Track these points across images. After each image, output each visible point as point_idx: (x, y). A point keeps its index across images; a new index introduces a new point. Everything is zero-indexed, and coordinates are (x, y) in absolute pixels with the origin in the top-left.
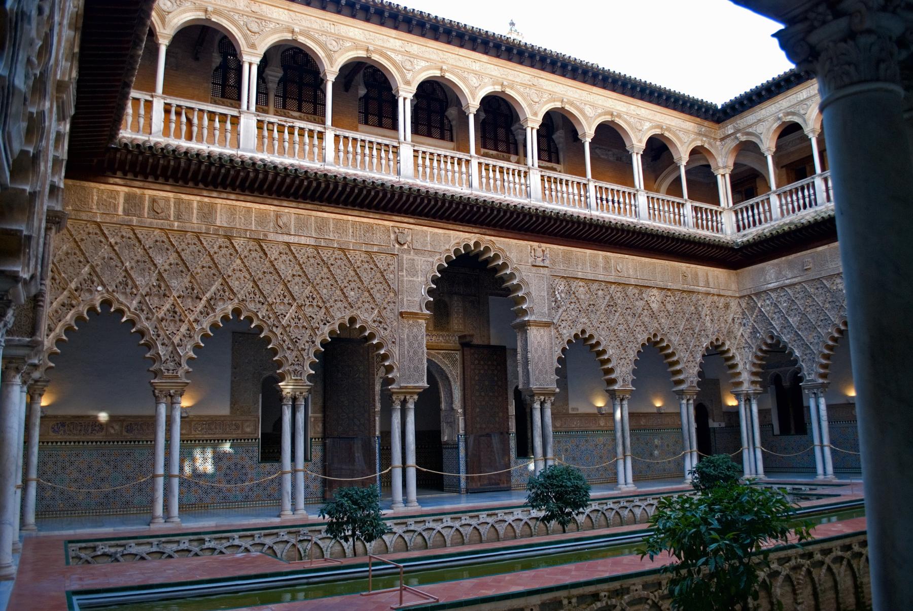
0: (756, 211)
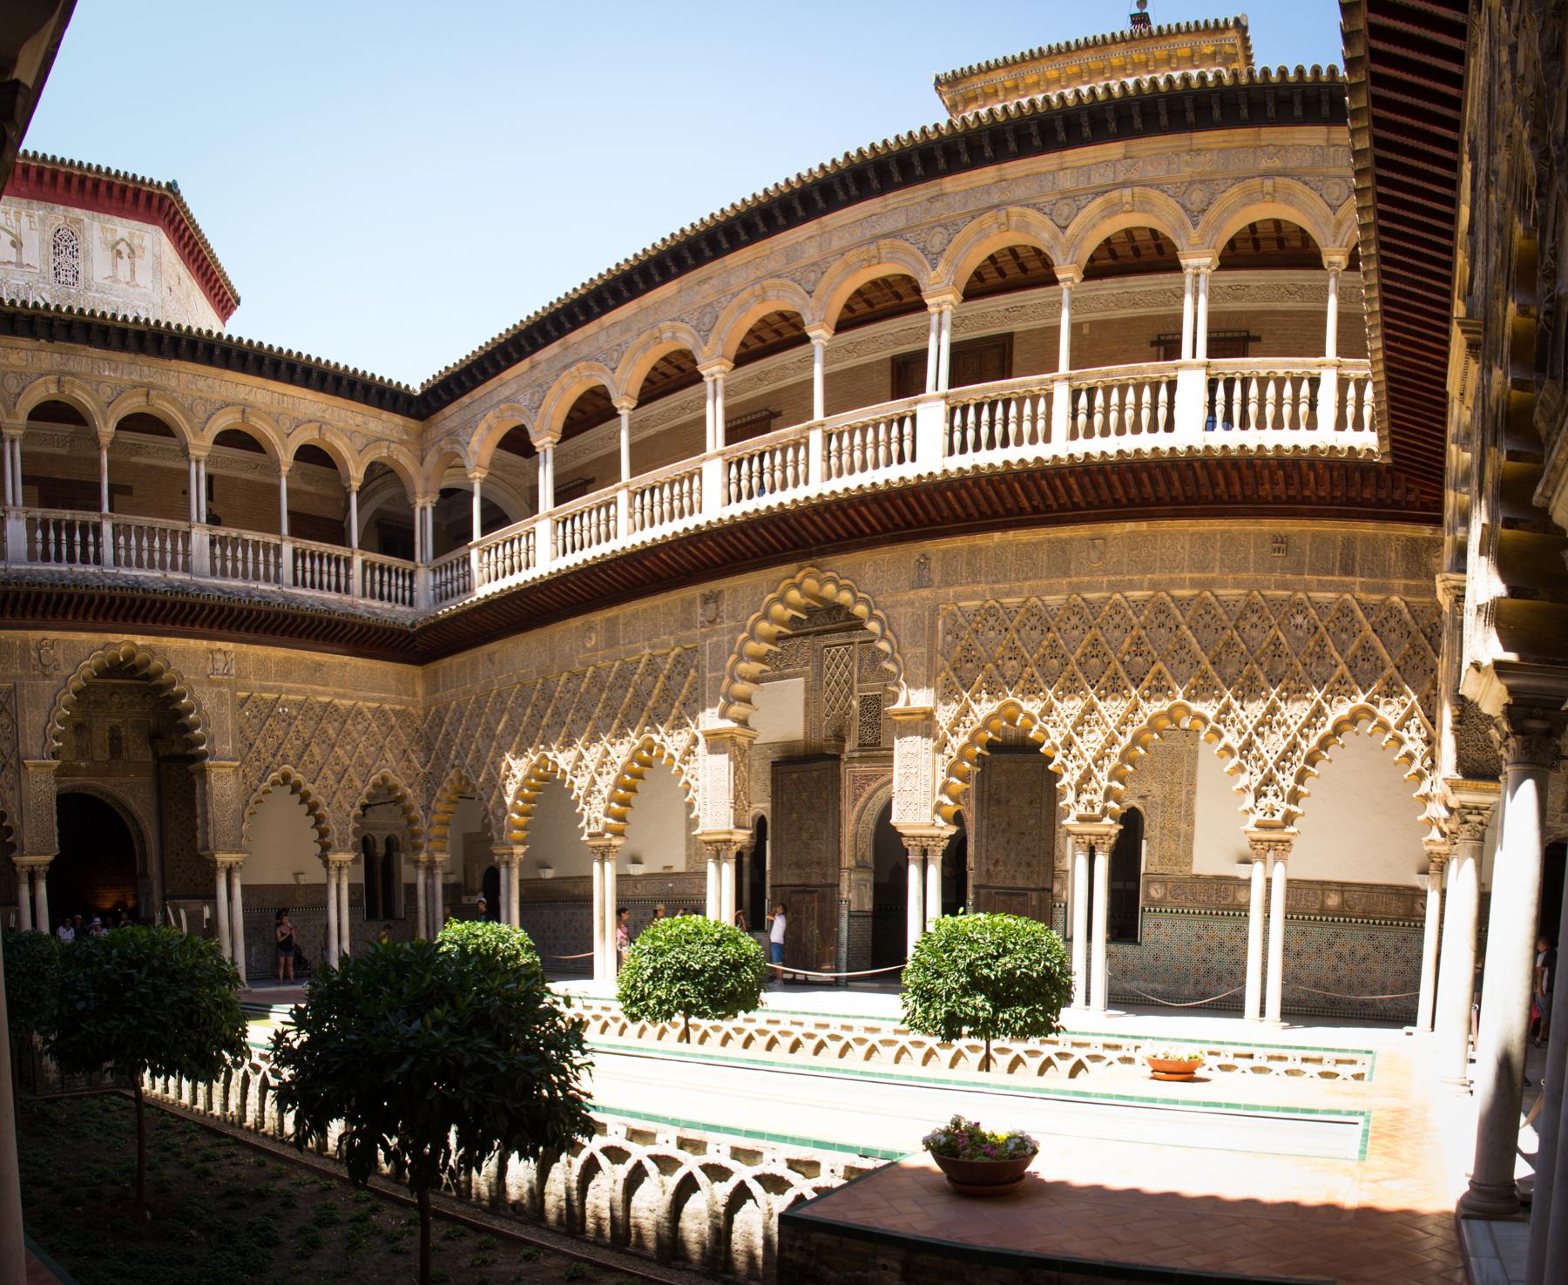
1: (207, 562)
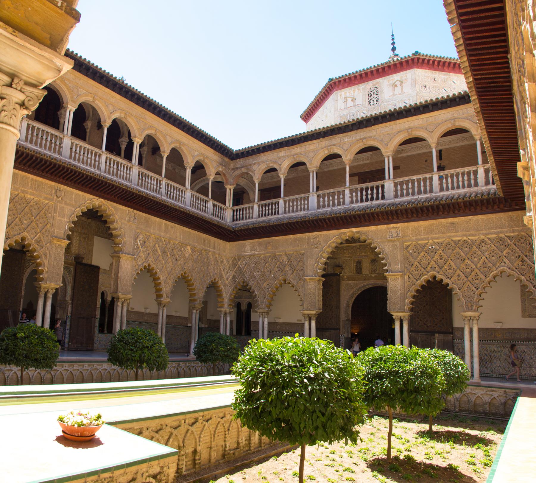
0: (245, 212)
1: (393, 194)
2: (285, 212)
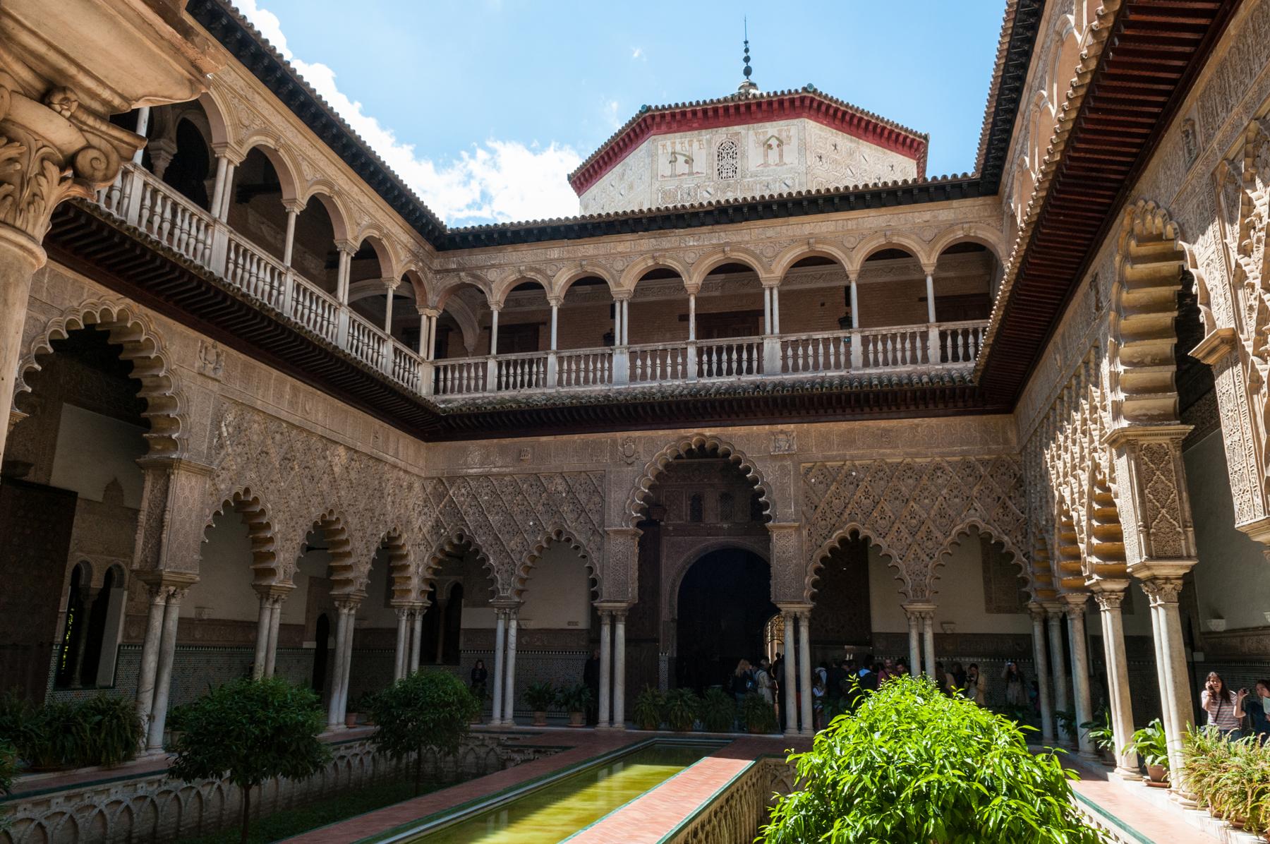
1: (779, 363)
2: (560, 383)
